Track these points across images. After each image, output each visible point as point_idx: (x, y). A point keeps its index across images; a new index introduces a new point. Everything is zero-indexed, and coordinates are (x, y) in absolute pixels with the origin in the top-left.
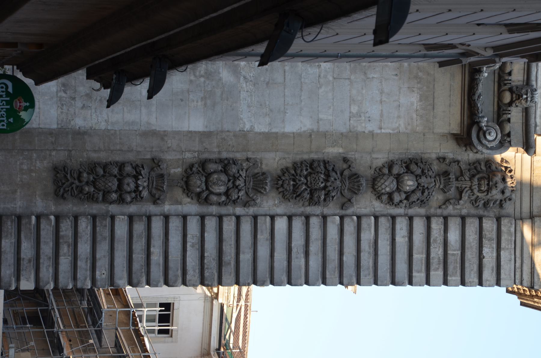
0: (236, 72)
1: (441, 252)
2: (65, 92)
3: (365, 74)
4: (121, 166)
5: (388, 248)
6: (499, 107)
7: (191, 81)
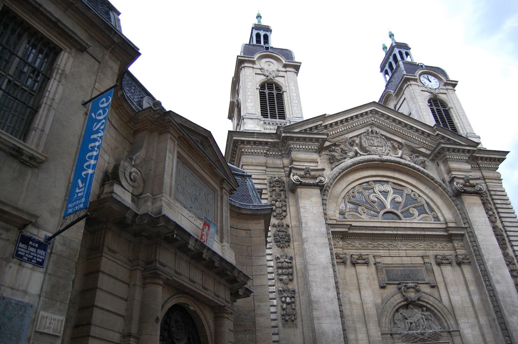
0: (488, 259)
1: (504, 205)
2: (515, 314)
3: (474, 222)
5: (509, 219)
6: (470, 186)
7: (496, 273)
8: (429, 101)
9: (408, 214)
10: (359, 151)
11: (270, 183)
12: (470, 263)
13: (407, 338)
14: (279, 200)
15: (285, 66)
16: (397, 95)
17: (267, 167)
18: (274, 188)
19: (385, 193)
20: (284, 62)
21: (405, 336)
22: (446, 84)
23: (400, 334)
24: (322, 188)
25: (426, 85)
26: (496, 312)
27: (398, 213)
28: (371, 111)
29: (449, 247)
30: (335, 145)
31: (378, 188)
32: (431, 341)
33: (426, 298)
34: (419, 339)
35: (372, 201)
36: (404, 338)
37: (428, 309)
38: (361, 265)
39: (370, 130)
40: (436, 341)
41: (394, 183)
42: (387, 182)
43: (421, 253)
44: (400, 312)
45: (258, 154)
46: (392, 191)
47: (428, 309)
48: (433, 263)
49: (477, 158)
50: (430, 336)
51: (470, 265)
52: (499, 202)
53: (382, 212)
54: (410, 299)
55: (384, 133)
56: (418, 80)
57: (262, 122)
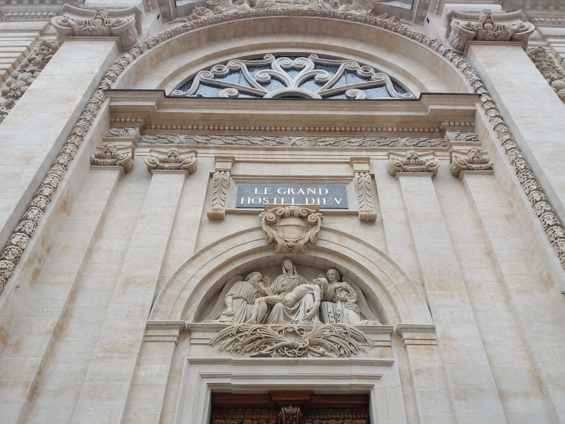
12: (490, 168)
13: (236, 340)
21: (233, 335)
23: (218, 328)
29: (433, 144)
32: (323, 355)
34: (275, 345)
35: (257, 81)
36: (229, 340)
38: (167, 173)
40: (341, 355)
41: (320, 56)
43: (347, 155)
44: (251, 279)
50: (321, 340)
51: (492, 174)
54: (280, 241)
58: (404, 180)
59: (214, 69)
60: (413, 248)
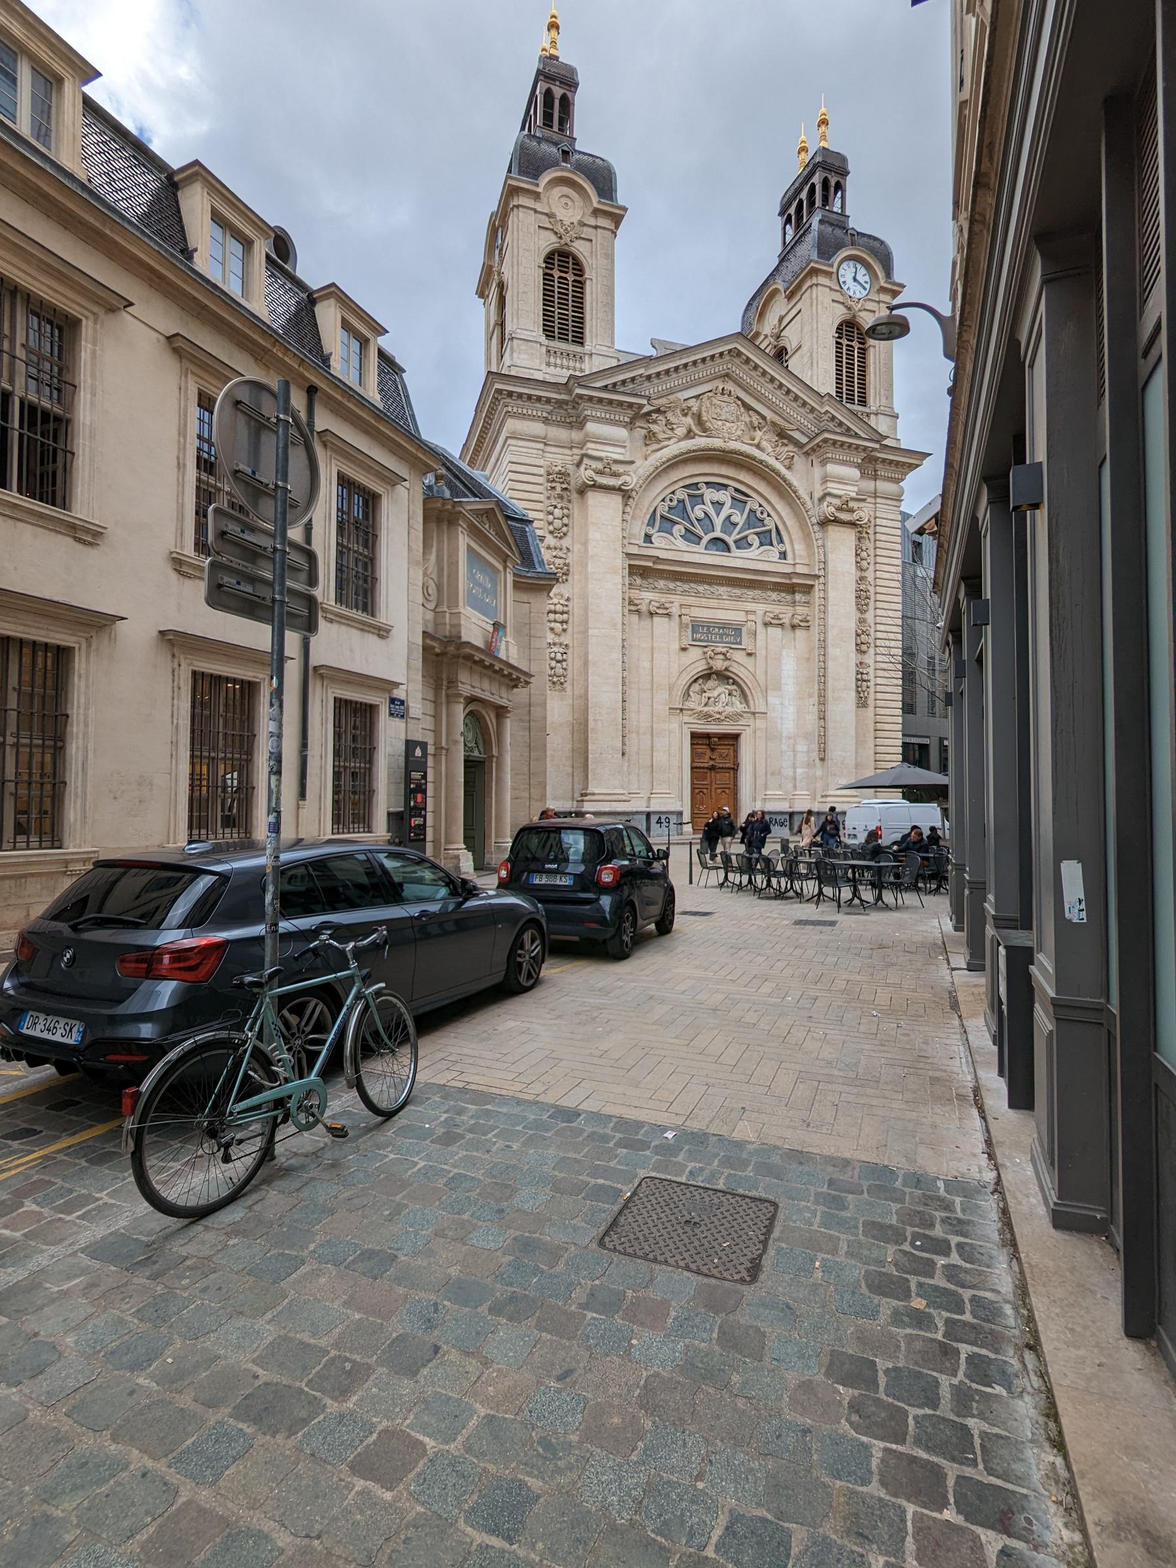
4: (857, 680)
8: (839, 329)
9: (742, 543)
10: (693, 428)
11: (549, 474)
14: (559, 506)
15: (596, 212)
16: (790, 297)
17: (546, 444)
18: (554, 485)
19: (718, 505)
20: (596, 205)
22: (883, 290)
24: (626, 494)
25: (845, 288)
26: (820, 696)
27: (730, 540)
28: (730, 351)
30: (658, 411)
31: (710, 495)
33: (735, 668)
37: (735, 683)
39: (720, 388)
41: (736, 490)
42: (725, 486)
45: (532, 418)
46: (729, 502)
47: (735, 683)
48: (759, 622)
49: (876, 459)
52: (883, 537)
53: (706, 538)
55: (742, 395)
56: (834, 276)
57: (544, 349)
58: (770, 629)
59: (667, 499)
60: (766, 672)
